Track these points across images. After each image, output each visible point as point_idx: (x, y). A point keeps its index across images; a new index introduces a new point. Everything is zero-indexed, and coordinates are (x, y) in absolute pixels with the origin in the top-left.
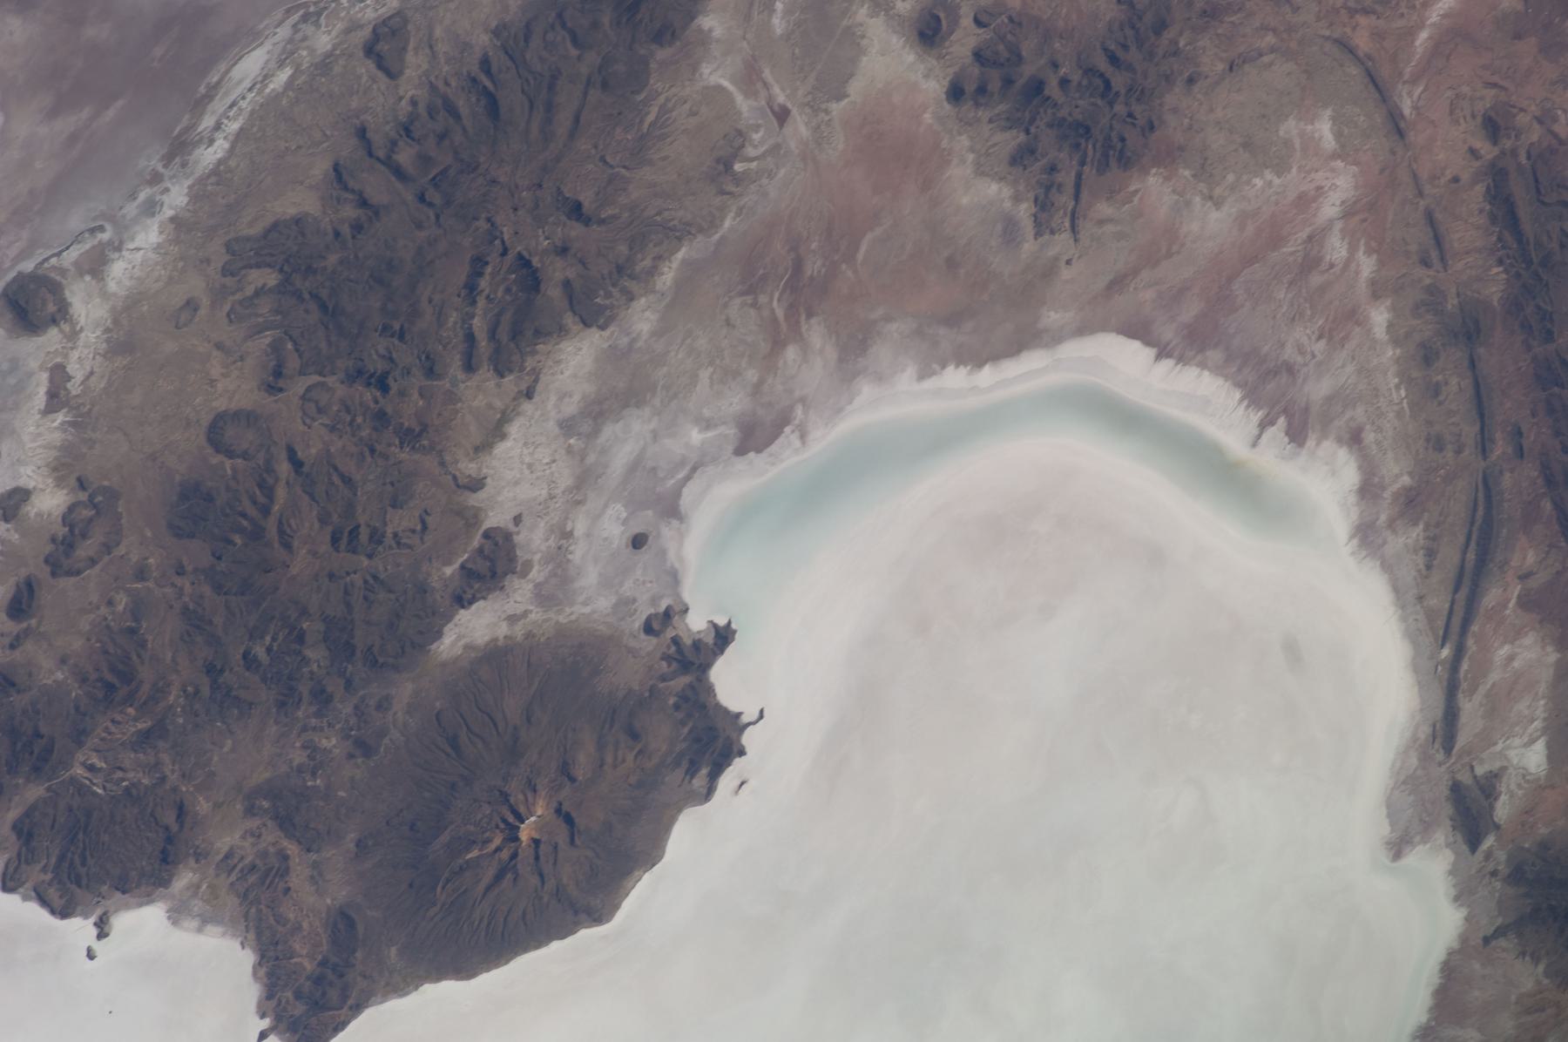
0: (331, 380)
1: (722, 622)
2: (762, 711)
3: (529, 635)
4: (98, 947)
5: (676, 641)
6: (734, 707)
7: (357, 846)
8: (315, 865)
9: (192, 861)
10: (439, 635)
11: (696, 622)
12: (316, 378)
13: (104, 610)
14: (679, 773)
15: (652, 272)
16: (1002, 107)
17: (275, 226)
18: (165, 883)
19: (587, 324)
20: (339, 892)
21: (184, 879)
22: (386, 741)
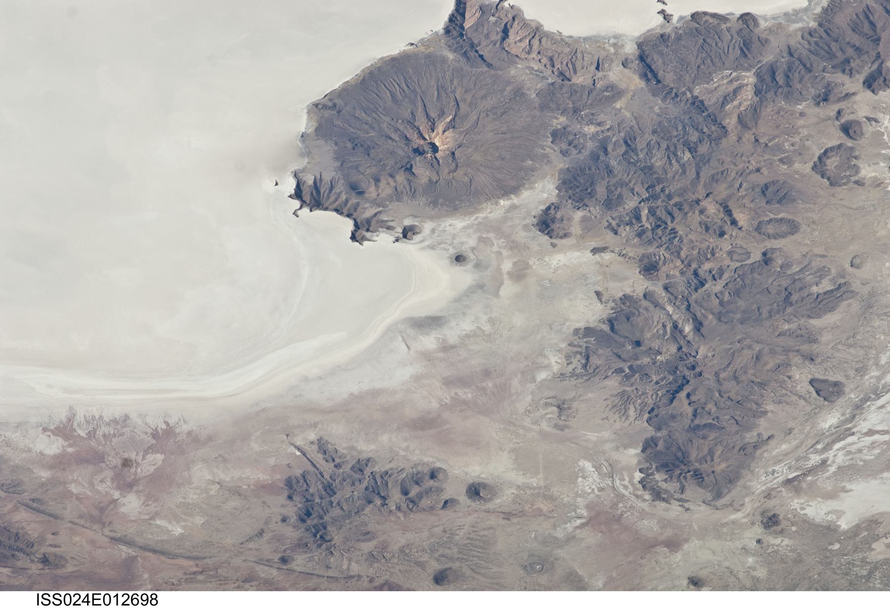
0: (738, 264)
1: (366, 243)
2: (297, 216)
3: (497, 203)
5: (389, 228)
6: (318, 213)
8: (544, 78)
11: (383, 240)
12: (748, 262)
14: (327, 177)
16: (404, 475)
17: (832, 309)
22: (551, 139)
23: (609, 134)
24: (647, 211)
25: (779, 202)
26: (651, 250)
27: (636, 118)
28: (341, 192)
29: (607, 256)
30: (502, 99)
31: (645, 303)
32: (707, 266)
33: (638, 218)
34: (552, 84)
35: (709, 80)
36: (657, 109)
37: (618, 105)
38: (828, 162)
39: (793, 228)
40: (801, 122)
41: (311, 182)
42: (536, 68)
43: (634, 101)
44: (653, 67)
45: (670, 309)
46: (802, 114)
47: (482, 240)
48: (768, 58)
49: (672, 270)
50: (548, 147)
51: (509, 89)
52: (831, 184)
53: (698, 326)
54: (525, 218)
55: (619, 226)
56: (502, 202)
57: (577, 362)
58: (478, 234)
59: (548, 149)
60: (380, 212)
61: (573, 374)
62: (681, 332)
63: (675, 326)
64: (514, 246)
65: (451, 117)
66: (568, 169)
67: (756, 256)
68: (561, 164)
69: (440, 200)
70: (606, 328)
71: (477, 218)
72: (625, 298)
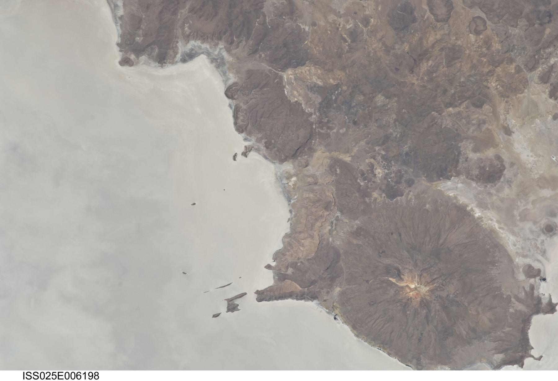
3: (480, 218)
4: (240, 157)
7: (357, 229)
9: (296, 163)
10: (449, 178)
14: (493, 345)
18: (282, 161)
20: (338, 241)
21: (288, 167)
22: (399, 198)
23: (379, 158)
24: (451, 109)
27: (357, 143)
28: (504, 332)
30: (366, 244)
34: (342, 212)
35: (298, 104)
37: (347, 159)
42: (330, 228)
44: (297, 149)
47: (524, 217)
48: (265, 67)
50: (409, 197)
51: (355, 242)
54: (490, 194)
55: (473, 125)
56: (478, 213)
58: (518, 223)
59: (410, 196)
64: (523, 192)
65: (390, 279)
66: (425, 177)
68: (423, 183)
69: (489, 260)
71: (500, 228)
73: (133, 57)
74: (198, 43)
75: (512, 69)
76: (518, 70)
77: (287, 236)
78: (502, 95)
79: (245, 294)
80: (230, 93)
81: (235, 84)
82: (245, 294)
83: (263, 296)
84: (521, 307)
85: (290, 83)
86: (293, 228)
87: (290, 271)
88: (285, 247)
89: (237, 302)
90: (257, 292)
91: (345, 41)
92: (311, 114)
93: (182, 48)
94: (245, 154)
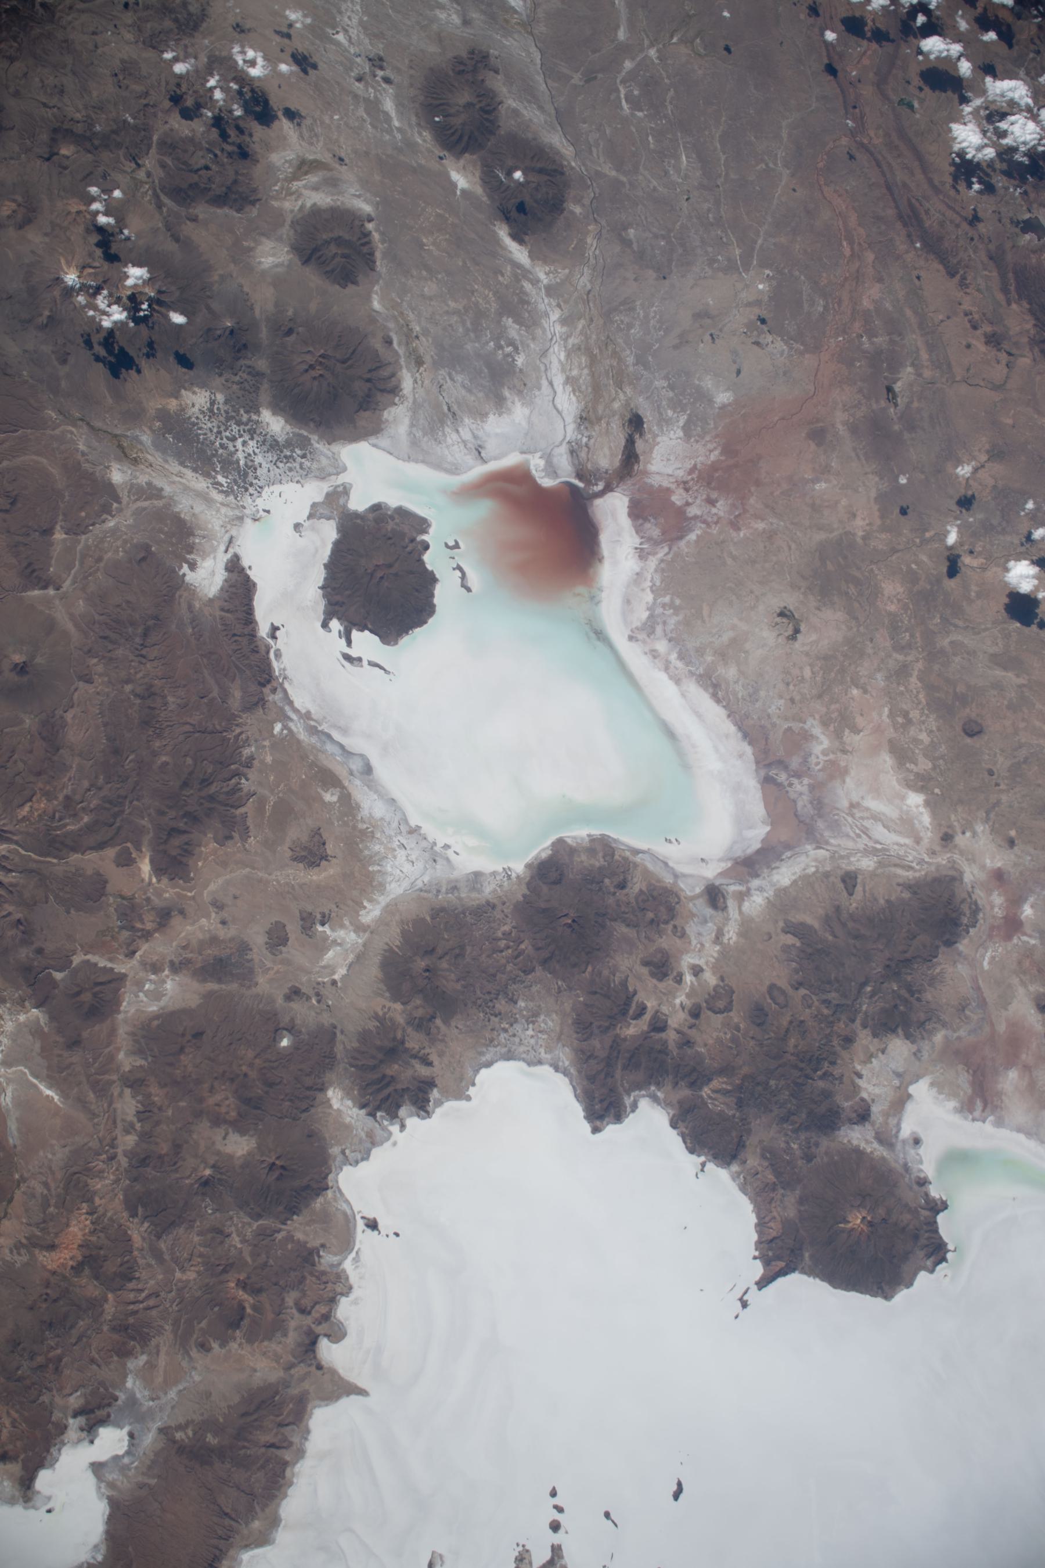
0: (813, 997)
1: (944, 1199)
3: (872, 1152)
5: (927, 1194)
6: (945, 1239)
11: (934, 1192)
12: (807, 992)
13: (721, 1034)
15: (931, 1033)
19: (907, 1039)
20: (791, 1213)
21: (735, 1167)
23: (789, 1133)
25: (762, 1010)
26: (838, 1048)
29: (858, 1067)
31: (870, 1023)
32: (826, 1011)
33: (825, 1074)
35: (722, 1111)
36: (758, 1122)
38: (722, 1007)
39: (772, 987)
40: (711, 1042)
41: (931, 1259)
43: (764, 1132)
45: (864, 1007)
46: (706, 1045)
49: (841, 1027)
51: (802, 1208)
52: (733, 992)
53: (864, 984)
56: (869, 1150)
57: (929, 1026)
60: (922, 1208)
61: (939, 1020)
62: (873, 991)
63: (871, 997)
67: (803, 991)
68: (825, 1143)
70: (900, 1031)
72: (875, 1035)
73: (598, 1123)
74: (637, 1093)
75: (842, 1025)
76: (847, 1025)
77: (757, 1225)
78: (844, 1048)
79: (748, 1289)
80: (674, 1125)
81: (674, 1116)
82: (748, 1289)
83: (763, 1283)
84: (925, 1213)
85: (710, 1098)
86: (758, 1217)
87: (770, 1253)
88: (759, 1237)
89: (745, 1298)
90: (757, 1283)
91: (731, 1048)
92: (734, 1116)
93: (628, 1101)
94: (702, 1170)
